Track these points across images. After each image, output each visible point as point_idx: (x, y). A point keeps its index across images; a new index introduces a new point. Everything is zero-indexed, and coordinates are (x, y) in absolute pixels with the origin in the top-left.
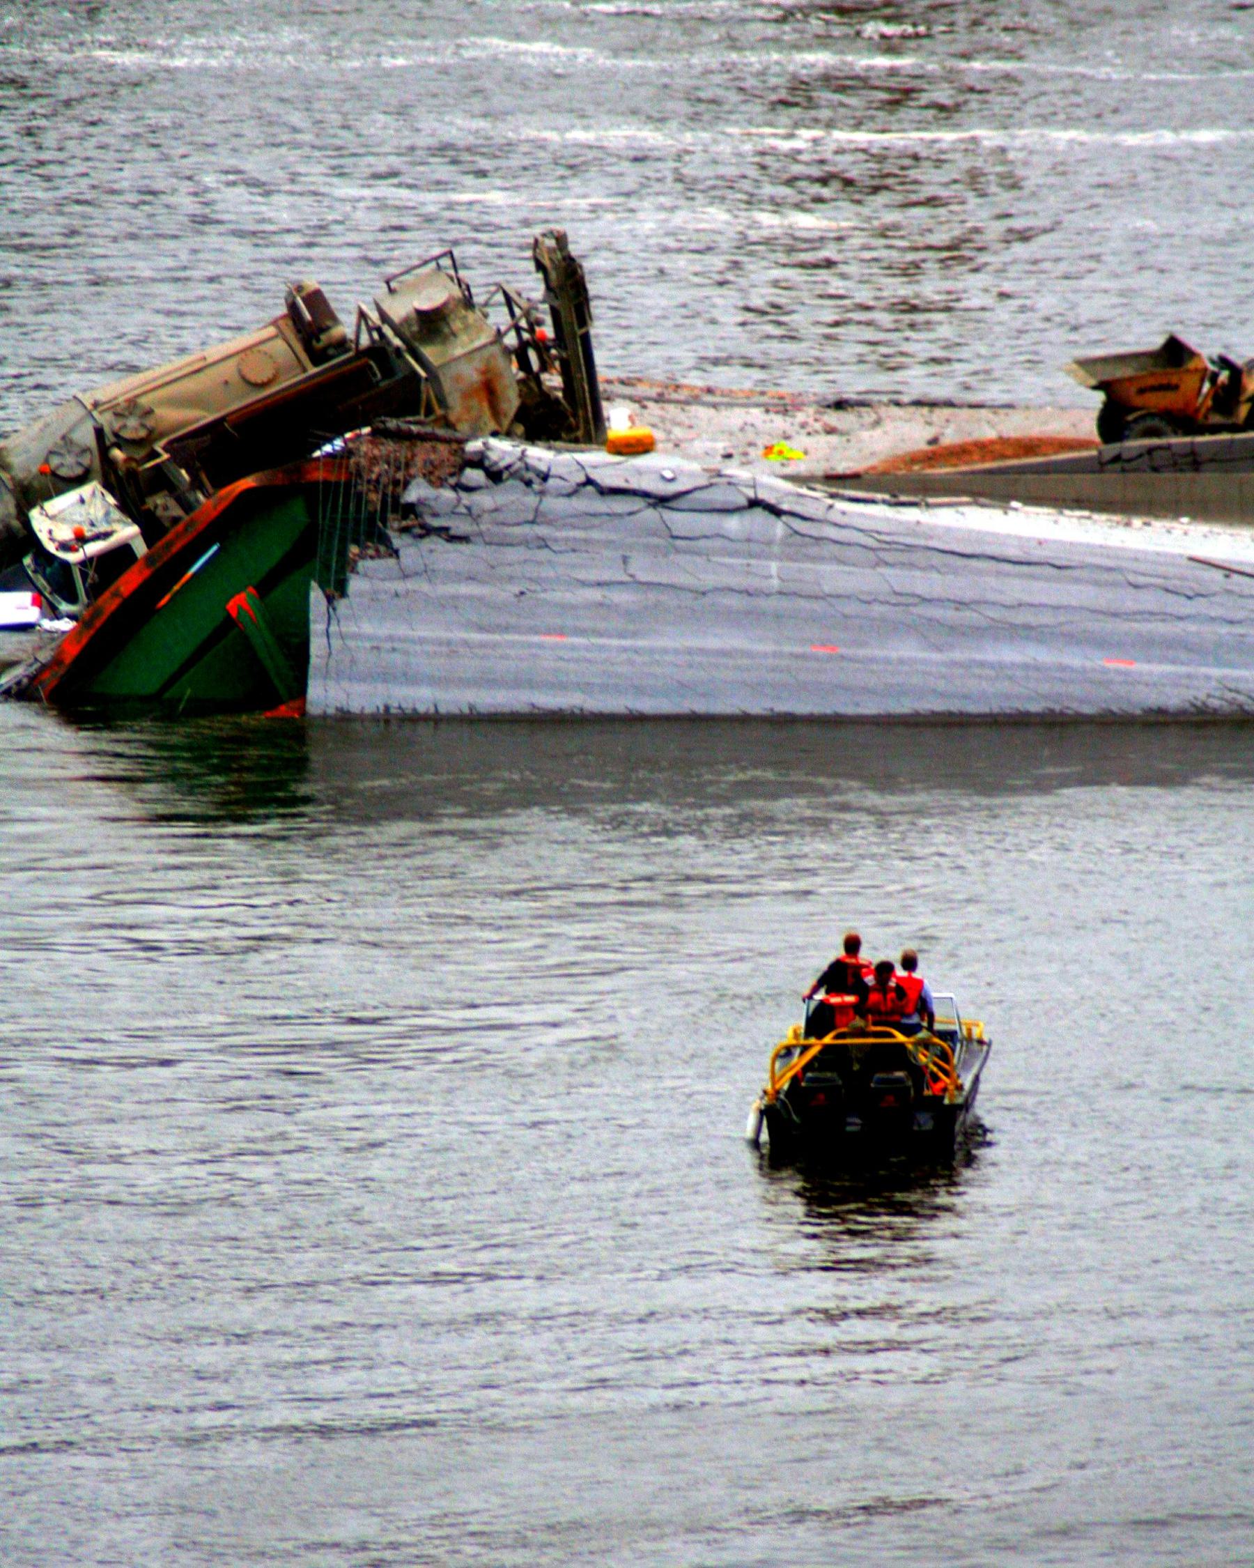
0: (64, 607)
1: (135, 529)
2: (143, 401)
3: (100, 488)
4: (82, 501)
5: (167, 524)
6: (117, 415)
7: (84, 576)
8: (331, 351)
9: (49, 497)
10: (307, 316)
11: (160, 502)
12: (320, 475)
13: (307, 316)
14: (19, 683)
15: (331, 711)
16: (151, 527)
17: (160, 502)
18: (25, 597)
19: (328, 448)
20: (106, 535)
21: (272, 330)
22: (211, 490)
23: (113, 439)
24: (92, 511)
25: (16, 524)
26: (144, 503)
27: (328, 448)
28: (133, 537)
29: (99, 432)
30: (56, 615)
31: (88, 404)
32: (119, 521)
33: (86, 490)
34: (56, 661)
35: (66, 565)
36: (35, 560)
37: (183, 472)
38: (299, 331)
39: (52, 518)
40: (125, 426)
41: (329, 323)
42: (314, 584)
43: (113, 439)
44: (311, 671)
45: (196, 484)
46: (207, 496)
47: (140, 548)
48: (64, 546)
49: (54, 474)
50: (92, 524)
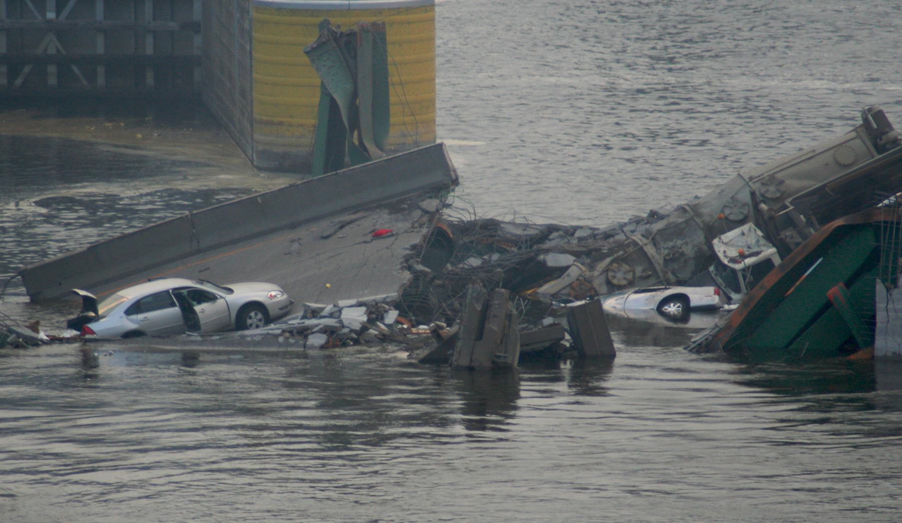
0: (735, 296)
1: (773, 250)
2: (779, 176)
3: (753, 226)
4: (743, 234)
5: (792, 247)
6: (763, 184)
7: (745, 277)
8: (888, 146)
9: (724, 232)
10: (875, 126)
11: (788, 234)
12: (882, 218)
13: (875, 126)
14: (706, 339)
15: (889, 354)
16: (784, 249)
17: (788, 234)
18: (711, 290)
19: (886, 202)
20: (757, 254)
21: (854, 134)
22: (817, 226)
23: (761, 198)
24: (749, 240)
25: (705, 248)
26: (779, 235)
27: (886, 202)
28: (773, 254)
29: (753, 194)
30: (729, 300)
31: (746, 177)
32: (764, 245)
33: (745, 228)
34: (728, 327)
35: (734, 271)
36: (716, 269)
37: (802, 216)
38: (870, 135)
39: (726, 244)
40: (768, 190)
41: (888, 130)
42: (878, 281)
43: (761, 198)
44: (877, 331)
45: (810, 223)
46: (816, 230)
47: (777, 261)
48: (733, 260)
49: (726, 218)
50: (749, 247)
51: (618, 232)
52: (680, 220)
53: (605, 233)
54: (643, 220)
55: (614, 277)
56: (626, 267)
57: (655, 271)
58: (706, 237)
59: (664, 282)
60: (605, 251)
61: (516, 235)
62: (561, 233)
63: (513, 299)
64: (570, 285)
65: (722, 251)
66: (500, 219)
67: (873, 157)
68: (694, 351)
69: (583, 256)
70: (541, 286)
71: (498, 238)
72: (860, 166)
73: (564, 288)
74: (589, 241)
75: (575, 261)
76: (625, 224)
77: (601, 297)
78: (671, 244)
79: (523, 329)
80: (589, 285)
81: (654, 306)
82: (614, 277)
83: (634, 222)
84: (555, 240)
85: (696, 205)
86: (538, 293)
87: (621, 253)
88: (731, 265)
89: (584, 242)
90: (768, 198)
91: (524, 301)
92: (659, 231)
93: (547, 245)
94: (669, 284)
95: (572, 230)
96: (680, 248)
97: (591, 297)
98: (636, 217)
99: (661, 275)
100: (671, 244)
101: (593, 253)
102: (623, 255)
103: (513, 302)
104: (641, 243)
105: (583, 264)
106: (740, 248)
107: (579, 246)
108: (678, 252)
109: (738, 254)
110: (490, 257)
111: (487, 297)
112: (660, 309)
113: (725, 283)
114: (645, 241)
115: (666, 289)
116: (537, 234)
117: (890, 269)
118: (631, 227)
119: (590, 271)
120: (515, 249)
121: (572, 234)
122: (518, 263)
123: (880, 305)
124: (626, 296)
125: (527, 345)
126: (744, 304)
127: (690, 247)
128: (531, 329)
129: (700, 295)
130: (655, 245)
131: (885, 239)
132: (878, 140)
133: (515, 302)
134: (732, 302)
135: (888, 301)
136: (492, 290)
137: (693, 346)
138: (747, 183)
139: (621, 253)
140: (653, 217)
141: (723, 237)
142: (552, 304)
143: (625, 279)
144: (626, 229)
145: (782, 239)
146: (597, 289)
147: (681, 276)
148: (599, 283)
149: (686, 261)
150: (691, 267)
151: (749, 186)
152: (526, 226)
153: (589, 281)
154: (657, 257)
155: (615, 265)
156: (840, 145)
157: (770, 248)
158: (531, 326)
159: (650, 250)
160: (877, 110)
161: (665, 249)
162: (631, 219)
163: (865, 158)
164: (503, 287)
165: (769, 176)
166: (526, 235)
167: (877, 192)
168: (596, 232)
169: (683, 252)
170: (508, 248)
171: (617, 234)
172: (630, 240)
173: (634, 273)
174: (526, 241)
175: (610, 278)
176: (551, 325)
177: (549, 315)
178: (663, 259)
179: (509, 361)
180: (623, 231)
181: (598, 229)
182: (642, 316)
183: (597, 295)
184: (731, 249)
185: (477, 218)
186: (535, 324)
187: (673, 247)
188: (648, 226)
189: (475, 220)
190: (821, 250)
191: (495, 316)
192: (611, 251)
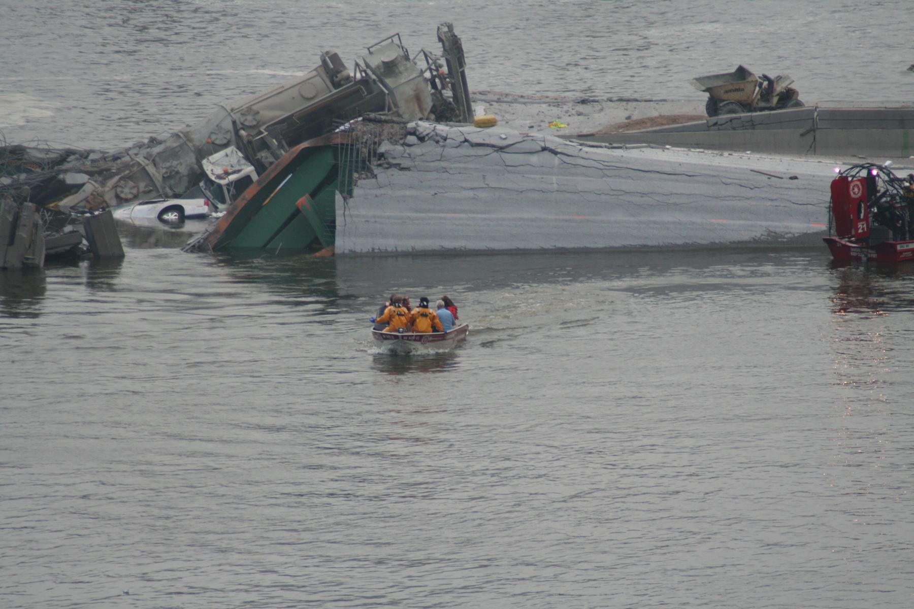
0: (220, 206)
1: (252, 168)
2: (255, 108)
3: (235, 149)
4: (227, 155)
5: (267, 165)
6: (242, 114)
7: (229, 190)
8: (342, 82)
9: (211, 154)
10: (331, 66)
11: (263, 155)
12: (339, 141)
13: (331, 66)
14: (199, 242)
15: (346, 251)
16: (260, 168)
17: (263, 155)
18: (201, 201)
19: (342, 128)
20: (239, 171)
21: (314, 73)
22: (288, 149)
23: (241, 126)
24: (232, 160)
25: (196, 167)
26: (256, 155)
27: (342, 128)
28: (251, 172)
29: (234, 123)
30: (216, 209)
31: (229, 109)
32: (244, 164)
33: (228, 150)
34: (216, 231)
35: (220, 186)
36: (205, 184)
37: (274, 140)
38: (327, 73)
39: (213, 164)
40: (246, 120)
41: (341, 69)
42: (337, 192)
43: (241, 126)
44: (337, 233)
45: (281, 146)
46: (286, 151)
47: (255, 177)
48: (219, 177)
49: (213, 143)
50: (232, 166)
51: (123, 155)
52: (175, 145)
53: (113, 156)
54: (144, 145)
55: (122, 192)
56: (131, 184)
57: (156, 186)
58: (197, 159)
59: (163, 196)
60: (114, 171)
61: (40, 159)
62: (77, 156)
63: (38, 210)
64: (86, 199)
65: (210, 170)
66: (26, 145)
67: (331, 91)
68: (189, 251)
69: (96, 175)
70: (61, 200)
71: (24, 161)
72: (321, 98)
73: (81, 201)
74: (101, 162)
75: (89, 179)
76: (130, 148)
77: (111, 209)
78: (168, 164)
79: (48, 236)
80: (102, 199)
81: (154, 215)
82: (122, 192)
83: (138, 146)
84: (72, 162)
85: (187, 133)
86: (59, 206)
87: (127, 172)
88: (217, 181)
89: (96, 164)
90: (246, 126)
91: (47, 213)
92: (158, 153)
93: (66, 166)
94: (167, 197)
95: (86, 154)
96: (175, 168)
97: (104, 209)
98: (139, 142)
99: (160, 190)
100: (168, 164)
101: (105, 172)
102: (129, 174)
103: (39, 213)
104: (143, 164)
105: (96, 181)
106: (224, 167)
107: (92, 167)
108: (174, 170)
109: (223, 172)
110: (18, 177)
111: (17, 210)
112: (160, 217)
113: (213, 195)
114: (147, 162)
115: (164, 201)
116: (57, 158)
117: (346, 182)
118: (135, 151)
119: (102, 187)
120: (39, 170)
121: (86, 157)
122: (43, 182)
123: (339, 212)
124: (132, 207)
125: (52, 249)
126: (229, 213)
127: (184, 166)
128: (54, 235)
129: (193, 206)
130: (155, 165)
131: (341, 158)
132: (335, 78)
133: (40, 213)
134: (219, 210)
135: (345, 208)
136: (21, 204)
137: (187, 247)
138: (229, 114)
139: (127, 172)
140: (153, 142)
141: (210, 158)
142: (71, 215)
143: (130, 193)
144: (130, 152)
145: (258, 159)
146: (108, 201)
147: (177, 191)
148: (109, 197)
149: (180, 178)
150: (185, 183)
151: (231, 116)
152: (48, 151)
153: (101, 195)
154: (157, 175)
155: (122, 182)
156: (304, 81)
157: (249, 166)
158: (54, 233)
159: (151, 169)
160: (333, 53)
161: (163, 168)
162: (134, 144)
163: (323, 92)
164: (31, 201)
165: (246, 108)
166: (48, 158)
167: (334, 120)
168: (106, 155)
169: (178, 171)
170: (33, 169)
171: (124, 157)
172: (134, 162)
173: (138, 188)
174: (48, 163)
175: (119, 193)
176: (71, 232)
177: (69, 224)
178: (161, 177)
179: (37, 262)
180: (128, 154)
181: (108, 153)
182: (146, 223)
183: (108, 206)
184: (217, 167)
185: (7, 145)
186: (57, 231)
187: (170, 167)
188: (148, 150)
189: (6, 146)
190: (292, 166)
191: (24, 225)
192: (119, 171)
